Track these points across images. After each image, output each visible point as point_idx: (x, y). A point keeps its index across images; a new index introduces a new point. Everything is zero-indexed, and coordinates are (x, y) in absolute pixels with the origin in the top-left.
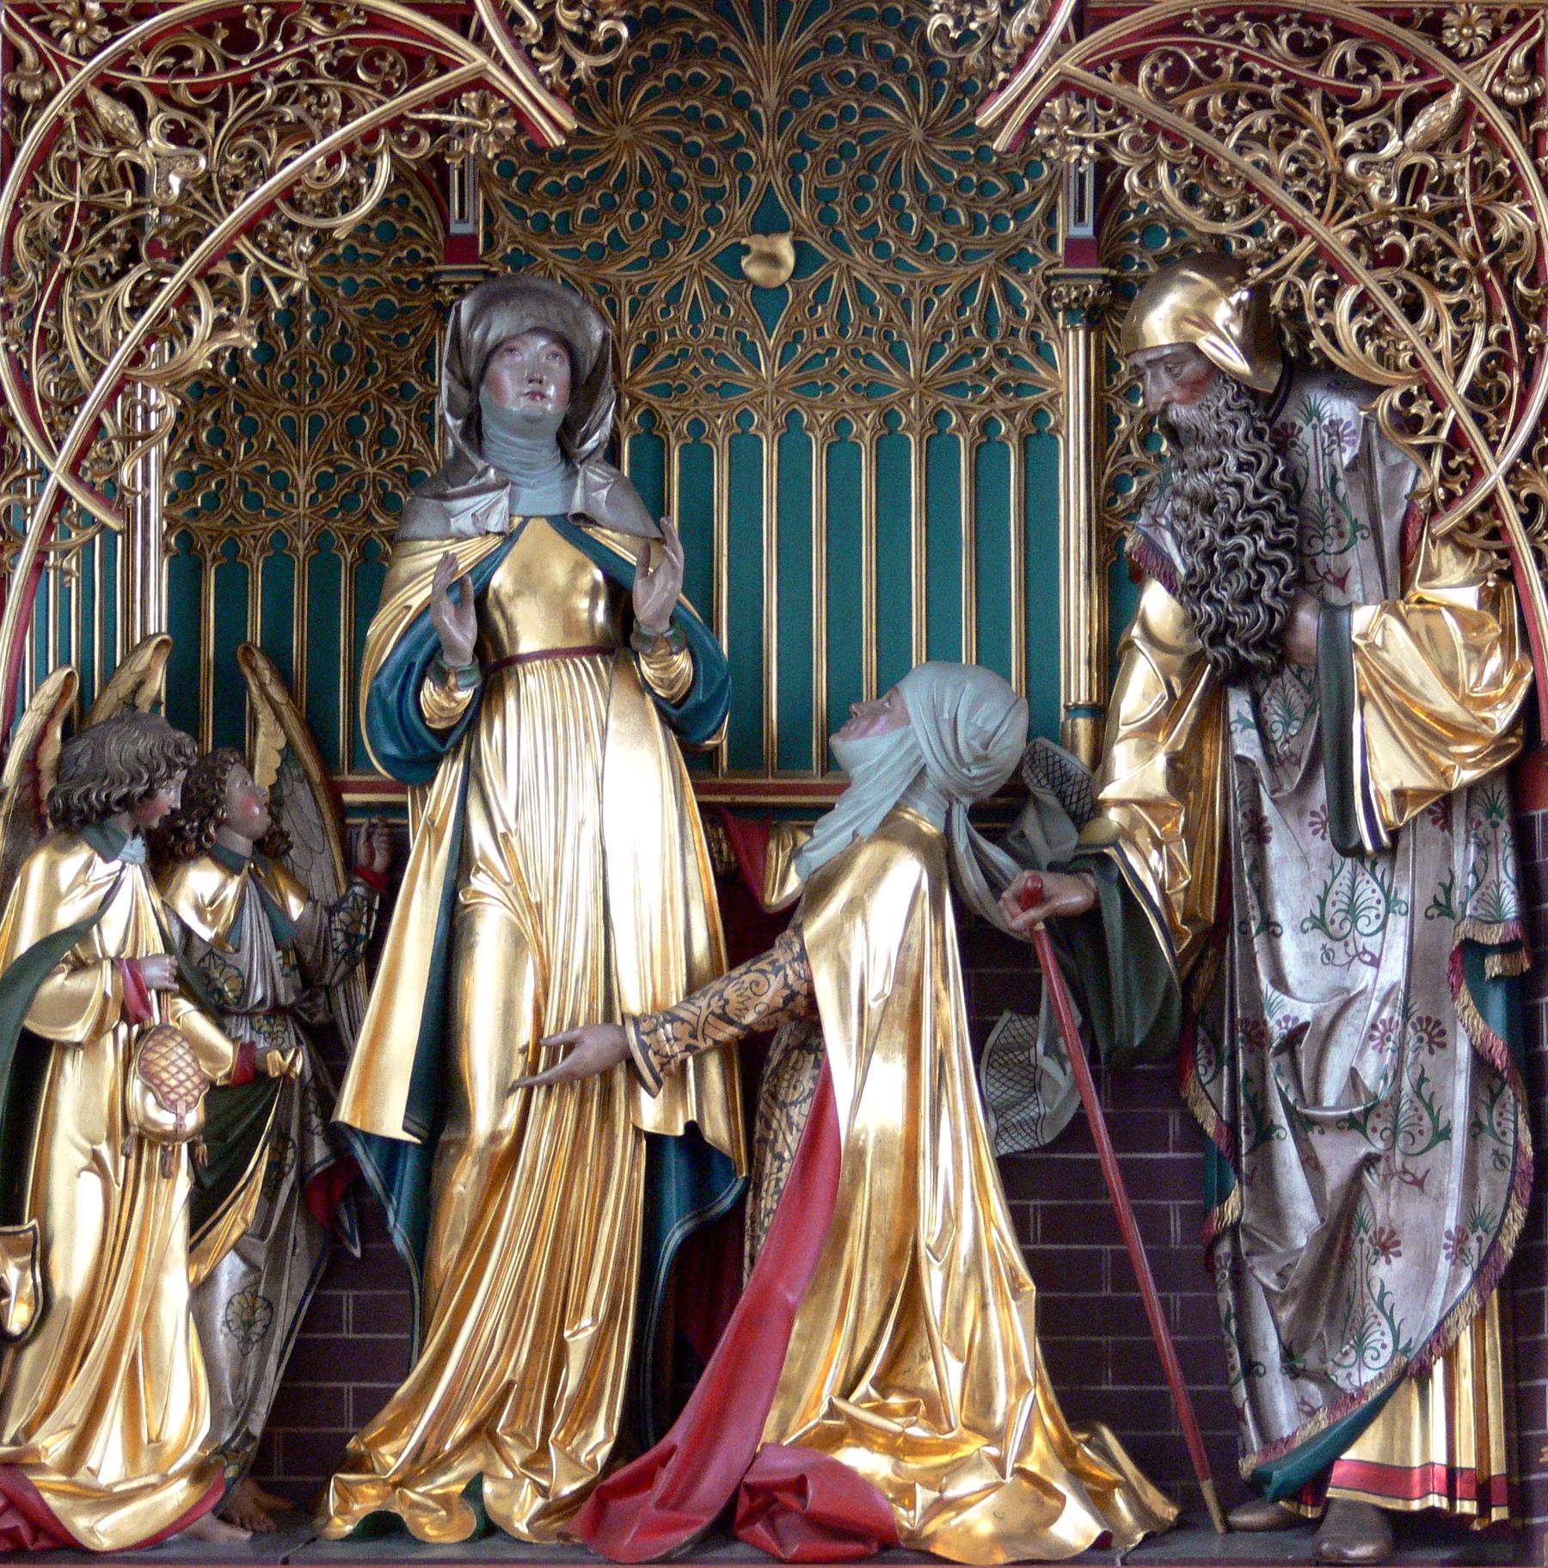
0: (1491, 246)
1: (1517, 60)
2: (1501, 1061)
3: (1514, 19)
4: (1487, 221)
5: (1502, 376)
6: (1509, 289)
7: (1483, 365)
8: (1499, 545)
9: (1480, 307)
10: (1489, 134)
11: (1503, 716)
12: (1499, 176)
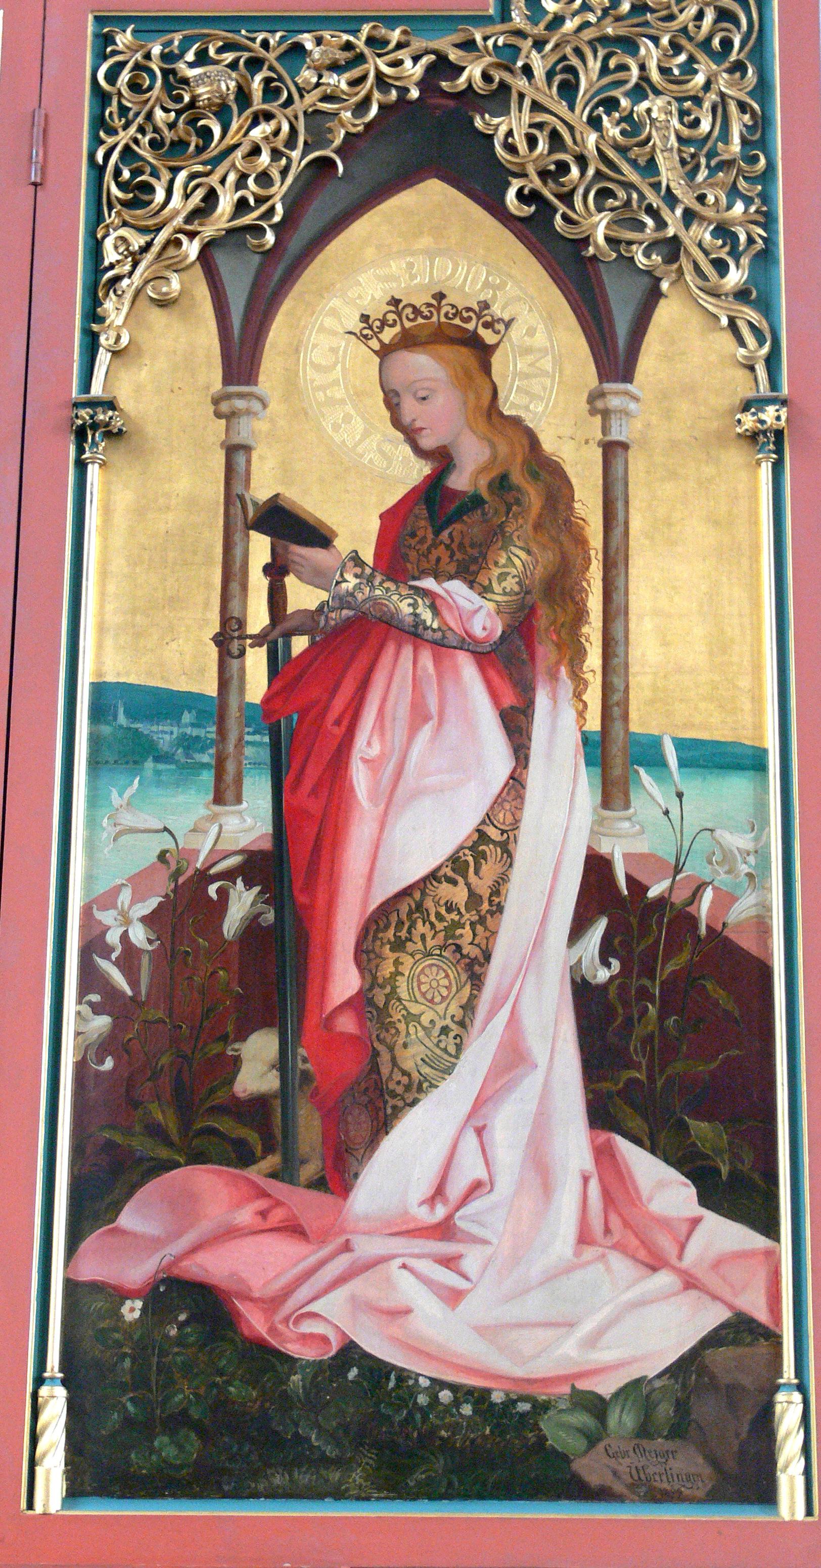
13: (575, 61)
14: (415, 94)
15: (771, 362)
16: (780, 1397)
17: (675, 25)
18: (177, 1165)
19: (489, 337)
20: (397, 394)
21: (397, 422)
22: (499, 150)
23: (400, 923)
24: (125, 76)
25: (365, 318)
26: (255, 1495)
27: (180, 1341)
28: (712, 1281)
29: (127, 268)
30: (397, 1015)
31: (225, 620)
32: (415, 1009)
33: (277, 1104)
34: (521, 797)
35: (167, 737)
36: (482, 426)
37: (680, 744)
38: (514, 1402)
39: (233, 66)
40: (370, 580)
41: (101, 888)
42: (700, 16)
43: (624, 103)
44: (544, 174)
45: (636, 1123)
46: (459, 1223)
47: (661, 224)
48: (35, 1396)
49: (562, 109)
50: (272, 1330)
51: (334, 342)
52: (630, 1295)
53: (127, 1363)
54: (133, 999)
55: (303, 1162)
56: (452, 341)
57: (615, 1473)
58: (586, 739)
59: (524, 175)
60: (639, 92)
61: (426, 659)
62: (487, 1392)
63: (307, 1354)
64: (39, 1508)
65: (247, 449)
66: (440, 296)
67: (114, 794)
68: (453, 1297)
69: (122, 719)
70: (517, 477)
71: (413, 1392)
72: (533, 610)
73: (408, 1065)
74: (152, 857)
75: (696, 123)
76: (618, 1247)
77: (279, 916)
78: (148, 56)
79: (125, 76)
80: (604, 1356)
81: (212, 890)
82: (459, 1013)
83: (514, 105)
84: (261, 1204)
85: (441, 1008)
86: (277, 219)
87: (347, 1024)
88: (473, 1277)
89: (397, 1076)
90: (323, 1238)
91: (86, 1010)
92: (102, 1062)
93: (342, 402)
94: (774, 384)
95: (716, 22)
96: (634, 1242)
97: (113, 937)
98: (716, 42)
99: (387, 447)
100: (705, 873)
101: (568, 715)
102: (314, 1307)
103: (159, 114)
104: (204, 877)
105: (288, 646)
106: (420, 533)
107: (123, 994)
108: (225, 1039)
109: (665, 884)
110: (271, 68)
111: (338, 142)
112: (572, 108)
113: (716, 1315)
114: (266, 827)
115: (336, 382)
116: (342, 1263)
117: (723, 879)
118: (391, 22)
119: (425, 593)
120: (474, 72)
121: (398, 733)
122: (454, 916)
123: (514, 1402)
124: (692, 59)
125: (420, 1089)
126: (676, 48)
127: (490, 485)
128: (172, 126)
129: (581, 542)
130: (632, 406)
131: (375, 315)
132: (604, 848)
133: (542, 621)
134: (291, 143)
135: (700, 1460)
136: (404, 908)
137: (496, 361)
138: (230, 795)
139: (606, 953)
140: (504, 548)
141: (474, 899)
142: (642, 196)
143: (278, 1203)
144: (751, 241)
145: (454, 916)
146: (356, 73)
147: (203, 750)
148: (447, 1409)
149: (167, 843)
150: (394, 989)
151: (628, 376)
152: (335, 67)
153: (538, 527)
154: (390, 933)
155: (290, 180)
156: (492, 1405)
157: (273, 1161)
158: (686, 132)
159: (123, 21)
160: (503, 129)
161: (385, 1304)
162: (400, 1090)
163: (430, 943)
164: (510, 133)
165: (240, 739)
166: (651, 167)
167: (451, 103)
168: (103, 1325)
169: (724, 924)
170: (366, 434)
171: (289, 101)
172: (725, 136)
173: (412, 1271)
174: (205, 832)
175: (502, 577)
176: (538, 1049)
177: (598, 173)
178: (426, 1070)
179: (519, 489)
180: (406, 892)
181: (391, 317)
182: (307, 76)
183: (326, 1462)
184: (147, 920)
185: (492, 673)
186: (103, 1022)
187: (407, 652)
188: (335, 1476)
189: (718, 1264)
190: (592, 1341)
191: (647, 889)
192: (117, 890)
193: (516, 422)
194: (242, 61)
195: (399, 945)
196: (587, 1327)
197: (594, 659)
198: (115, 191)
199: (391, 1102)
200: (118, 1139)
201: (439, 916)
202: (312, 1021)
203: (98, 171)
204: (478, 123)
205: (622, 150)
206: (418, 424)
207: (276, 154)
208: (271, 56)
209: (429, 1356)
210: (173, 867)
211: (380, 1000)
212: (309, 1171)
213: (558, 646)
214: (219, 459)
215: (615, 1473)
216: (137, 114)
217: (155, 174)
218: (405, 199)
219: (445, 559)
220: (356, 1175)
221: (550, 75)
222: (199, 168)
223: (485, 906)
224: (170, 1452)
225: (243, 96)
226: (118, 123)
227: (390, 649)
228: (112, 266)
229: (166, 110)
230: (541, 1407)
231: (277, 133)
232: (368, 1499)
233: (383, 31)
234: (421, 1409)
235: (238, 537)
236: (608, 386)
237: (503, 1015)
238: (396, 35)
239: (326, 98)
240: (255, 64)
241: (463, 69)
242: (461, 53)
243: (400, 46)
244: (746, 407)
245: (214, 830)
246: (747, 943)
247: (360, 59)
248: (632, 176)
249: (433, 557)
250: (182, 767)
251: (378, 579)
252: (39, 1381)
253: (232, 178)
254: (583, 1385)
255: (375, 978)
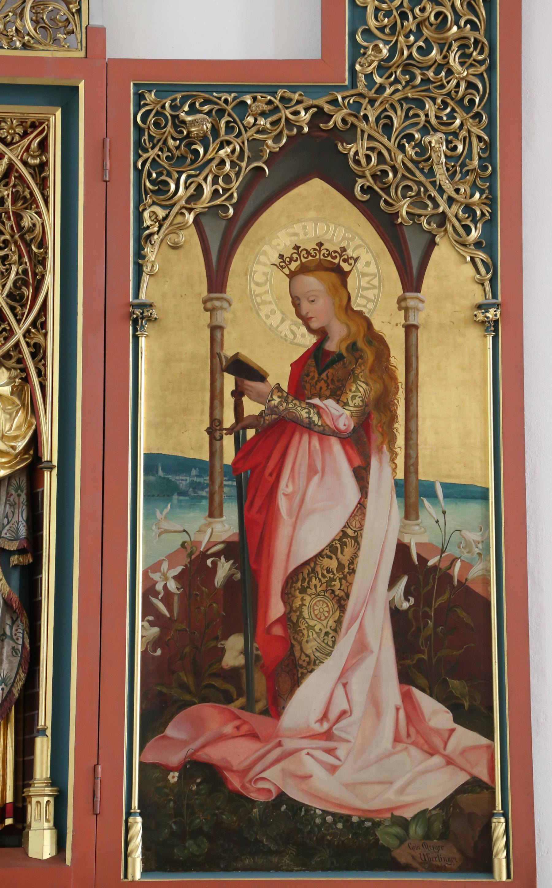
0: (20, 228)
1: (35, 145)
2: (16, 604)
3: (34, 126)
4: (19, 217)
5: (24, 289)
6: (30, 252)
7: (15, 283)
8: (21, 366)
9: (15, 258)
10: (20, 177)
11: (21, 445)
12: (25, 198)
13: (391, 113)
14: (306, 129)
15: (493, 281)
16: (494, 820)
17: (444, 91)
18: (194, 704)
19: (346, 267)
20: (299, 299)
21: (299, 314)
22: (351, 163)
23: (304, 579)
24: (151, 119)
25: (281, 256)
26: (236, 869)
27: (197, 793)
28: (460, 761)
29: (156, 229)
30: (303, 627)
31: (212, 420)
32: (312, 623)
33: (244, 671)
34: (364, 514)
35: (184, 483)
36: (343, 317)
37: (445, 486)
38: (363, 822)
39: (209, 113)
40: (286, 399)
41: (152, 562)
42: (458, 85)
43: (417, 136)
44: (374, 176)
45: (422, 681)
46: (335, 732)
47: (436, 205)
48: (127, 822)
49: (385, 140)
50: (243, 786)
51: (266, 269)
52: (420, 768)
53: (172, 804)
54: (170, 619)
55: (257, 701)
56: (326, 269)
57: (413, 857)
58: (397, 483)
59: (363, 177)
60: (426, 130)
61: (315, 442)
62: (350, 817)
63: (261, 798)
64: (130, 878)
65: (221, 328)
66: (320, 244)
67: (158, 512)
68: (333, 769)
69: (161, 473)
70: (361, 344)
71: (315, 815)
72: (369, 415)
73: (309, 652)
74: (178, 545)
75: (456, 147)
76: (414, 743)
77: (243, 575)
78: (163, 107)
79: (151, 119)
80: (407, 798)
81: (209, 562)
82: (334, 625)
83: (359, 137)
84: (237, 723)
85: (325, 623)
86: (235, 200)
87: (278, 631)
88: (342, 758)
89: (303, 657)
90: (267, 741)
91: (146, 624)
92: (155, 651)
93: (270, 303)
94: (495, 296)
95: (466, 88)
96: (421, 741)
97: (159, 587)
98: (466, 101)
99: (294, 328)
100: (457, 553)
101: (388, 470)
102: (264, 775)
103: (171, 142)
104: (204, 556)
105: (245, 435)
106: (311, 374)
107: (165, 616)
108: (217, 639)
109: (437, 559)
110: (229, 115)
111: (266, 157)
112: (389, 140)
113: (462, 778)
114: (235, 529)
115: (266, 292)
116: (277, 752)
117: (466, 556)
118: (293, 89)
119: (314, 406)
120: (337, 118)
121: (302, 482)
122: (331, 575)
123: (363, 822)
124: (453, 110)
125: (315, 664)
126: (445, 104)
127: (347, 348)
128: (178, 148)
129: (394, 379)
130: (420, 305)
131: (287, 255)
132: (406, 540)
133: (374, 422)
134: (241, 157)
135: (455, 850)
136: (306, 572)
137: (351, 281)
138: (217, 512)
139: (407, 594)
140: (354, 382)
141: (341, 567)
142: (426, 190)
143: (245, 722)
144: (483, 214)
145: (331, 575)
146: (274, 118)
147: (203, 489)
148: (330, 825)
149: (186, 538)
150: (301, 612)
151: (418, 289)
152: (263, 114)
153: (371, 371)
154: (299, 584)
155: (241, 179)
156: (352, 823)
157: (241, 701)
158: (449, 153)
159: (149, 88)
160: (353, 151)
161: (299, 773)
162: (305, 664)
163: (319, 589)
164: (356, 153)
165: (222, 483)
166: (431, 173)
167: (325, 135)
168: (159, 785)
169: (466, 579)
170: (283, 321)
171: (239, 134)
172: (470, 156)
173: (312, 756)
174: (205, 532)
175: (354, 397)
176: (373, 642)
177: (403, 175)
178: (318, 654)
179: (361, 350)
180: (307, 563)
181: (295, 256)
182: (251, 120)
183: (271, 852)
184: (175, 578)
185: (348, 448)
186: (156, 630)
187: (306, 437)
188: (275, 859)
189: (464, 752)
190: (401, 791)
191: (428, 561)
192: (160, 563)
193: (360, 314)
194: (214, 112)
195: (303, 590)
196: (398, 785)
197: (400, 441)
198: (148, 184)
199: (301, 670)
200: (164, 690)
201: (324, 576)
202: (260, 630)
203: (139, 173)
204: (340, 147)
205: (416, 163)
206: (310, 315)
207: (233, 164)
208: (229, 108)
209: (321, 799)
210: (189, 551)
211: (294, 619)
212: (260, 706)
213: (382, 434)
214: (208, 332)
215: (413, 857)
216: (159, 141)
217: (169, 175)
218: (302, 189)
219: (324, 388)
220: (284, 708)
221: (378, 119)
222: (192, 172)
223: (346, 570)
224: (194, 849)
225: (215, 130)
226: (149, 145)
227: (297, 436)
228: (148, 228)
229: (174, 139)
230: (377, 824)
231: (233, 151)
232: (292, 871)
233: (288, 94)
234: (317, 826)
235: (218, 376)
236: (408, 294)
237: (356, 625)
238: (296, 97)
239: (258, 132)
240: (221, 112)
241: (332, 116)
242: (332, 108)
243: (299, 102)
244: (479, 307)
245: (209, 531)
246: (478, 589)
247: (276, 110)
248: (422, 178)
249: (318, 387)
250: (193, 498)
251: (291, 398)
252: (129, 814)
253: (210, 179)
254: (397, 813)
255: (291, 607)
